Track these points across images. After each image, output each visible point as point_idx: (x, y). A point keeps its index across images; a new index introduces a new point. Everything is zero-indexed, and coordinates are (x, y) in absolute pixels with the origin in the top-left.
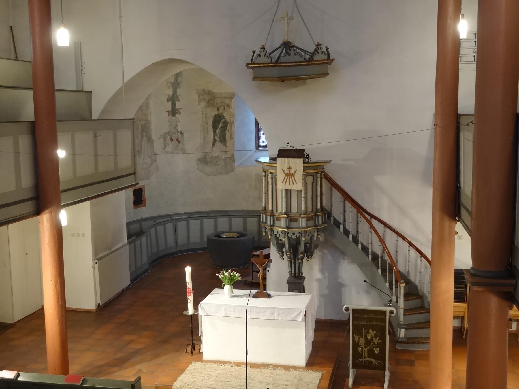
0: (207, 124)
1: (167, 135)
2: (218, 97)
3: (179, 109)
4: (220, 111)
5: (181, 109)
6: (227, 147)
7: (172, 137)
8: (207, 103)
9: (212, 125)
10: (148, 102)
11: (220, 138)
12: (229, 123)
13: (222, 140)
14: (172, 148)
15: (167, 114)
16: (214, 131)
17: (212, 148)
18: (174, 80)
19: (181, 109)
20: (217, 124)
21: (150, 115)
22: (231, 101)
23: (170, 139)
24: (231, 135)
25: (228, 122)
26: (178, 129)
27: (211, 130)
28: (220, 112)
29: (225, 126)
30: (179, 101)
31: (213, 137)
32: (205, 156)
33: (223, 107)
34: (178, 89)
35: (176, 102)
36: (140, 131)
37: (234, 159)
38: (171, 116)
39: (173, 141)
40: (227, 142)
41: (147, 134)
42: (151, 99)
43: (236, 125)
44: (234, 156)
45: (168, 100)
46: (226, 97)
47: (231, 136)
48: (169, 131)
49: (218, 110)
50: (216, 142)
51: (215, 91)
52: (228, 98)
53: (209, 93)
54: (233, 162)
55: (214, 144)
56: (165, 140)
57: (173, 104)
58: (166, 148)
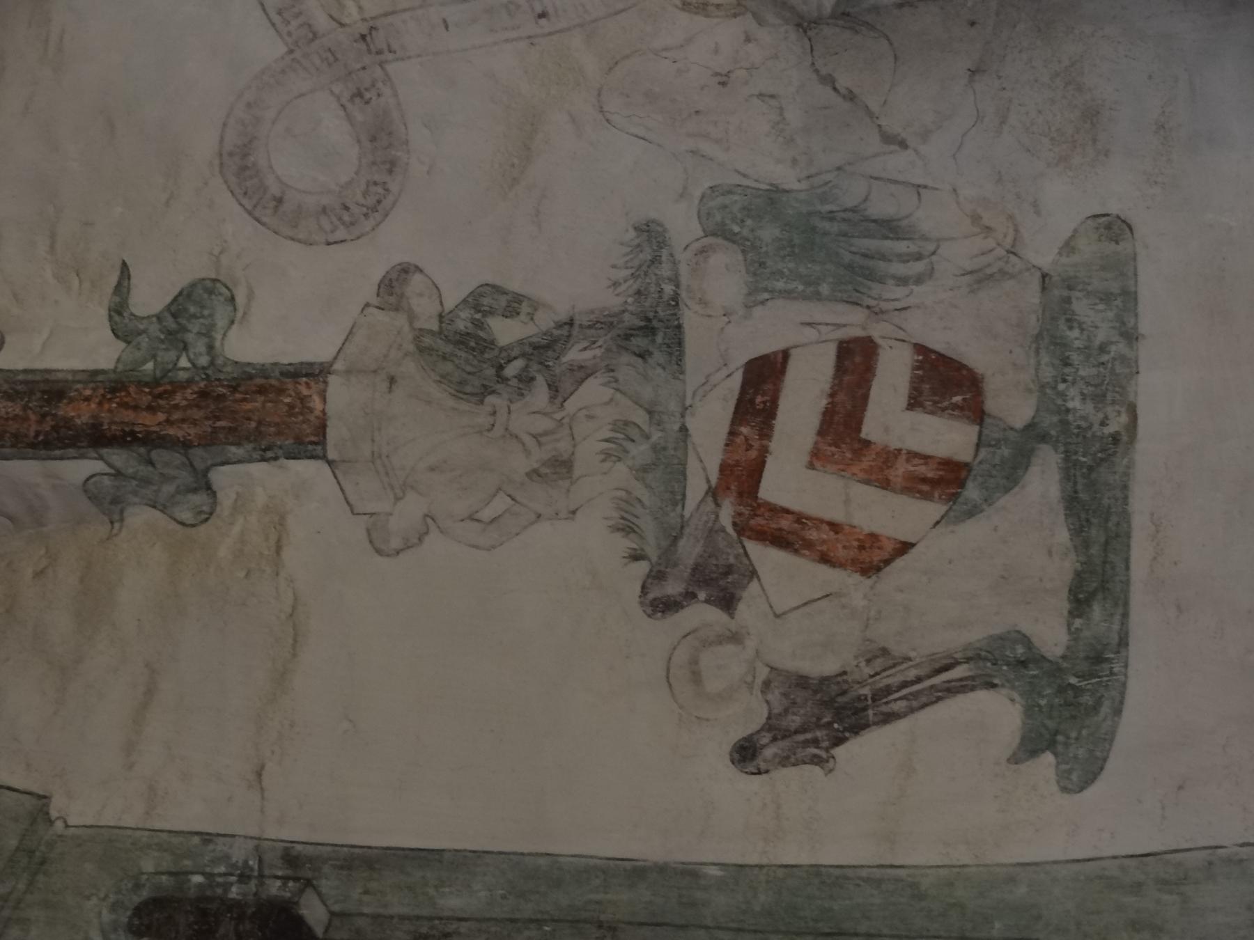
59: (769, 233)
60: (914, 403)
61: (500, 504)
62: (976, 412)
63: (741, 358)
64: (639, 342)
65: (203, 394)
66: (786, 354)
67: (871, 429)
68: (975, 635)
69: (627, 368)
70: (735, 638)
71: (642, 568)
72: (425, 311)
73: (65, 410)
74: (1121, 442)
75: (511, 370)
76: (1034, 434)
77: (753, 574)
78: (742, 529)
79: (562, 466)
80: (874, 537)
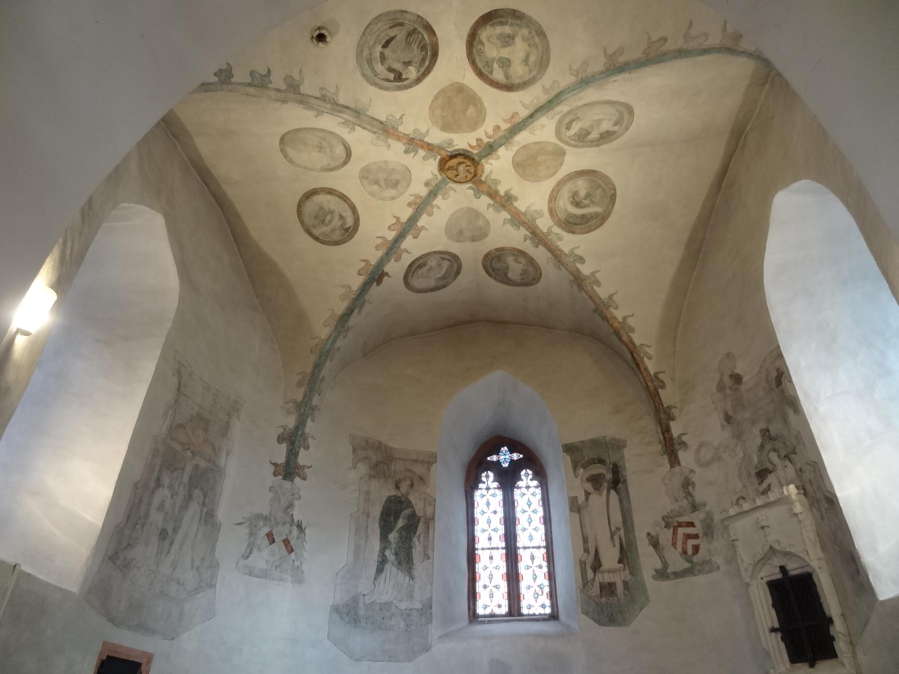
0: (368, 517)
1: (261, 523)
2: (400, 459)
3: (304, 467)
4: (401, 489)
5: (309, 467)
6: (413, 579)
7: (274, 532)
8: (373, 468)
9: (380, 520)
10: (228, 422)
11: (396, 554)
12: (422, 519)
13: (402, 559)
14: (267, 562)
16: (384, 536)
17: (375, 579)
18: (305, 396)
19: (309, 467)
20: (392, 518)
21: (227, 455)
22: (429, 470)
23: (267, 535)
24: (425, 548)
25: (421, 517)
26: (292, 515)
27: (378, 532)
28: (401, 492)
29: (411, 526)
30: (307, 448)
31: (380, 551)
32: (355, 600)
33: (409, 482)
34: (309, 420)
35: (300, 448)
36: (186, 479)
37: (431, 614)
38: (280, 477)
40: (414, 566)
41: (205, 498)
42: (239, 419)
43: (439, 525)
44: (431, 608)
45: (280, 439)
46: (416, 461)
47: (424, 551)
48: (268, 514)
49: (398, 487)
50: (386, 566)
51: (391, 444)
52: (422, 462)
53: (379, 447)
54: (429, 623)
55: (380, 570)
56: (252, 534)
57: (291, 450)
58: (252, 556)
59: (708, 521)
60: (693, 546)
61: (670, 493)
62: (694, 554)
63: (694, 521)
64: (693, 507)
65: (673, 451)
66: (695, 527)
67: (689, 541)
68: (668, 560)
69: (690, 506)
70: (662, 529)
71: (667, 514)
72: (690, 477)
73: (666, 433)
74: (694, 574)
75: (686, 490)
76: (692, 562)
77: (669, 529)
78: (674, 526)
79: (676, 500)
80: (676, 544)
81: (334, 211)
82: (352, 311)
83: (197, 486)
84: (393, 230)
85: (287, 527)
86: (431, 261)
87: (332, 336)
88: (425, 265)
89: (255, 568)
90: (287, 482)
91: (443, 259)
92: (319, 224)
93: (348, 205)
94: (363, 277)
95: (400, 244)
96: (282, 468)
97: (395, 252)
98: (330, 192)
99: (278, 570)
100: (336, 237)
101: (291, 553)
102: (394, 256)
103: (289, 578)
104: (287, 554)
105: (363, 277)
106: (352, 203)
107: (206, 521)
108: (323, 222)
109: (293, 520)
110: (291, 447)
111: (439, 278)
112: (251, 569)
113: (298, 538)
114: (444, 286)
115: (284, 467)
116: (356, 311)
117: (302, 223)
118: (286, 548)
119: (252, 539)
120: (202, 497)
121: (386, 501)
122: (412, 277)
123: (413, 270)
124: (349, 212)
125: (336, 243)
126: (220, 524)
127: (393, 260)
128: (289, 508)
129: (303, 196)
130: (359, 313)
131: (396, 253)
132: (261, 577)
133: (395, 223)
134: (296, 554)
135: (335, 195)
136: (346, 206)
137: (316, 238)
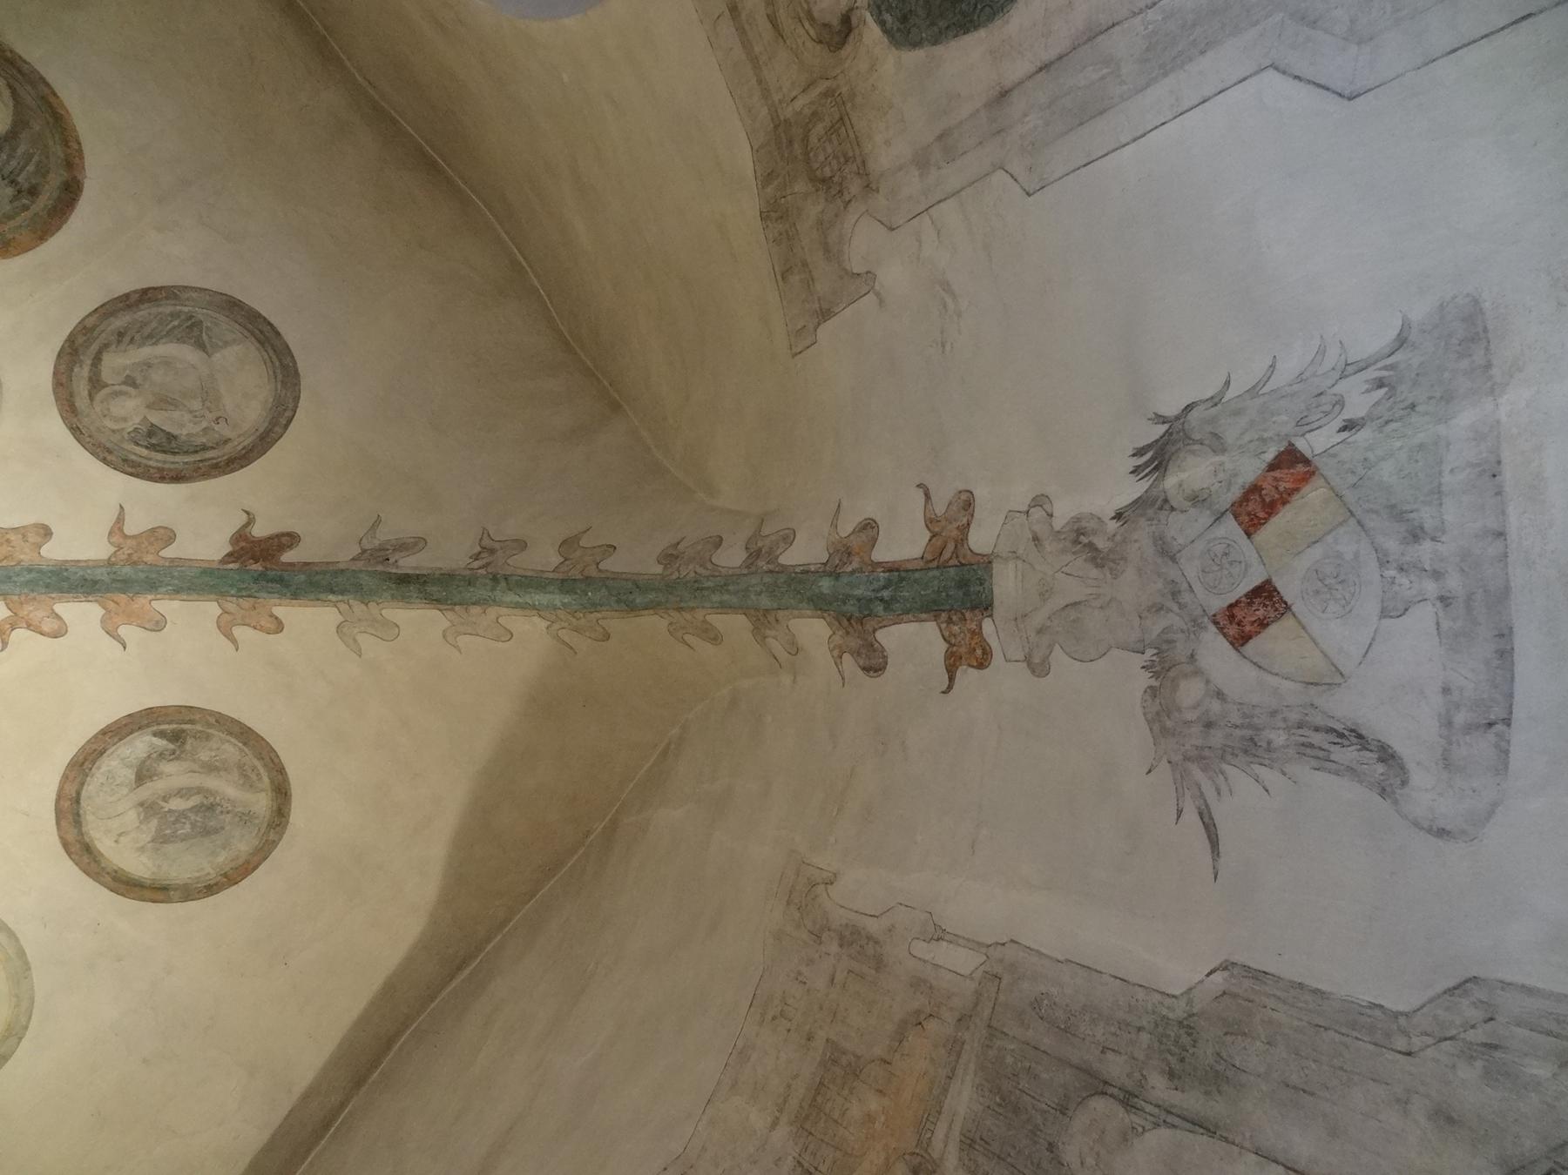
1: (1190, 692)
2: (766, 94)
3: (930, 522)
5: (927, 496)
7: (1218, 604)
15: (973, 672)
19: (927, 496)
21: (938, 935)
23: (1240, 640)
26: (1118, 516)
38: (988, 627)
39: (1265, 593)
41: (1099, 1086)
48: (1139, 660)
51: (743, 159)
56: (1252, 748)
81: (141, 804)
82: (404, 580)
83: (1051, 1147)
84: (58, 617)
85: (1184, 527)
86: (125, 420)
87: (517, 599)
88: (152, 431)
89: (1446, 690)
90: (996, 590)
91: (96, 383)
92: (228, 813)
93: (82, 784)
94: (279, 611)
95: (96, 564)
96: (956, 629)
97: (135, 563)
98: (83, 853)
99: (1427, 517)
100: (231, 750)
101: (1307, 462)
102: (149, 558)
103: (1466, 418)
104: (1317, 481)
105: (279, 611)
106: (65, 778)
107: (1218, 1079)
108: (211, 807)
109: (1139, 504)
110: (879, 609)
111: (201, 346)
112: (1460, 718)
113: (1217, 444)
114: (232, 306)
115: (950, 621)
116: (408, 563)
117: (262, 852)
118: (1284, 499)
119: (1279, 738)
120: (1099, 1105)
121: (916, 45)
122: (227, 441)
123: (198, 457)
124: (104, 769)
125: (245, 734)
126: (1226, 966)
127: (169, 552)
128: (1091, 546)
129: (168, 900)
130: (415, 544)
131: (135, 558)
132: (1504, 635)
133: (29, 626)
134: (1304, 424)
135: (81, 833)
136: (90, 789)
137: (282, 792)
